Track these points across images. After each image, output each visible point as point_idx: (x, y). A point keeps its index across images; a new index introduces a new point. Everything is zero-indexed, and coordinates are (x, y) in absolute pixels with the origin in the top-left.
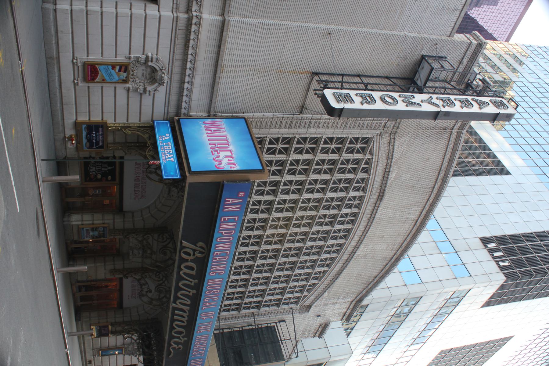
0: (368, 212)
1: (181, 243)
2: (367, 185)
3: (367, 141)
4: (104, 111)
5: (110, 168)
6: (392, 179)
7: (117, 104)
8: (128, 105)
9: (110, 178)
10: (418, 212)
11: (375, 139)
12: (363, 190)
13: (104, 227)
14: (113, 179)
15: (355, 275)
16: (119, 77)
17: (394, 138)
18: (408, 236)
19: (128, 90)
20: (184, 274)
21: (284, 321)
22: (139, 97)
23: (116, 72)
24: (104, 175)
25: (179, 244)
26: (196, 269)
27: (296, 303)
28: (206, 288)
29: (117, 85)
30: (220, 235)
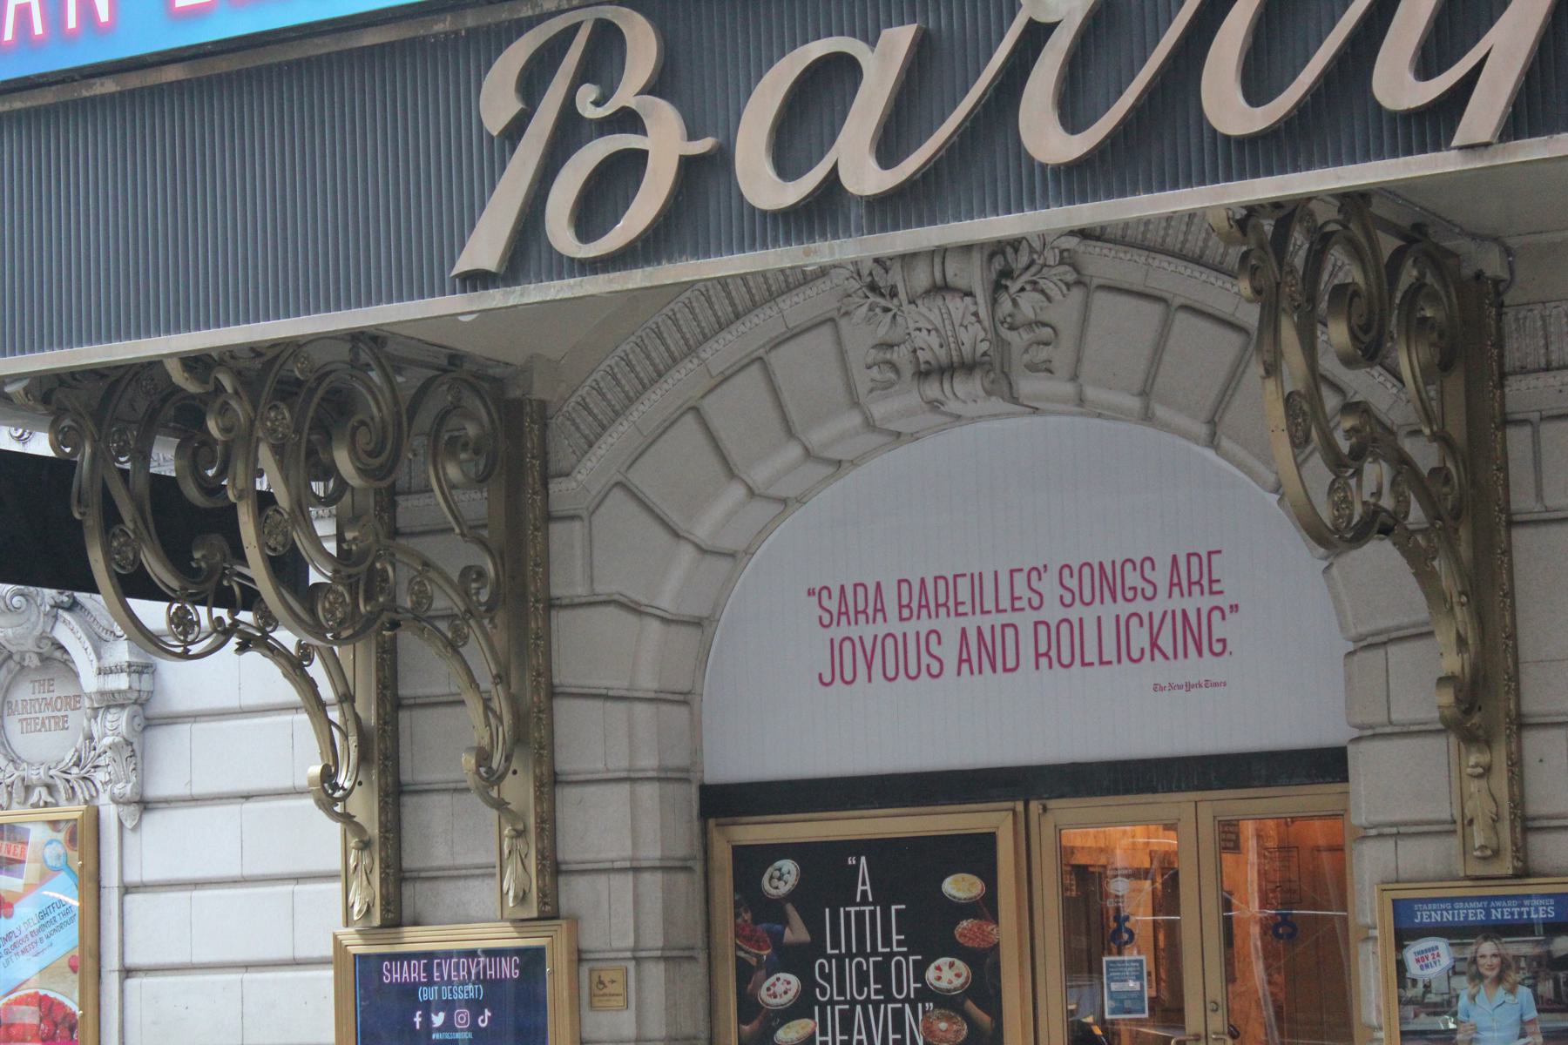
1: (477, 280)
4: (285, 953)
5: (864, 886)
7: (234, 871)
8: (247, 797)
9: (959, 887)
13: (1404, 934)
14: (976, 853)
16: (57, 870)
19: (144, 805)
20: (888, 148)
22: (183, 729)
23: (30, 888)
24: (932, 929)
25: (496, 298)
26: (817, 49)
29: (111, 878)
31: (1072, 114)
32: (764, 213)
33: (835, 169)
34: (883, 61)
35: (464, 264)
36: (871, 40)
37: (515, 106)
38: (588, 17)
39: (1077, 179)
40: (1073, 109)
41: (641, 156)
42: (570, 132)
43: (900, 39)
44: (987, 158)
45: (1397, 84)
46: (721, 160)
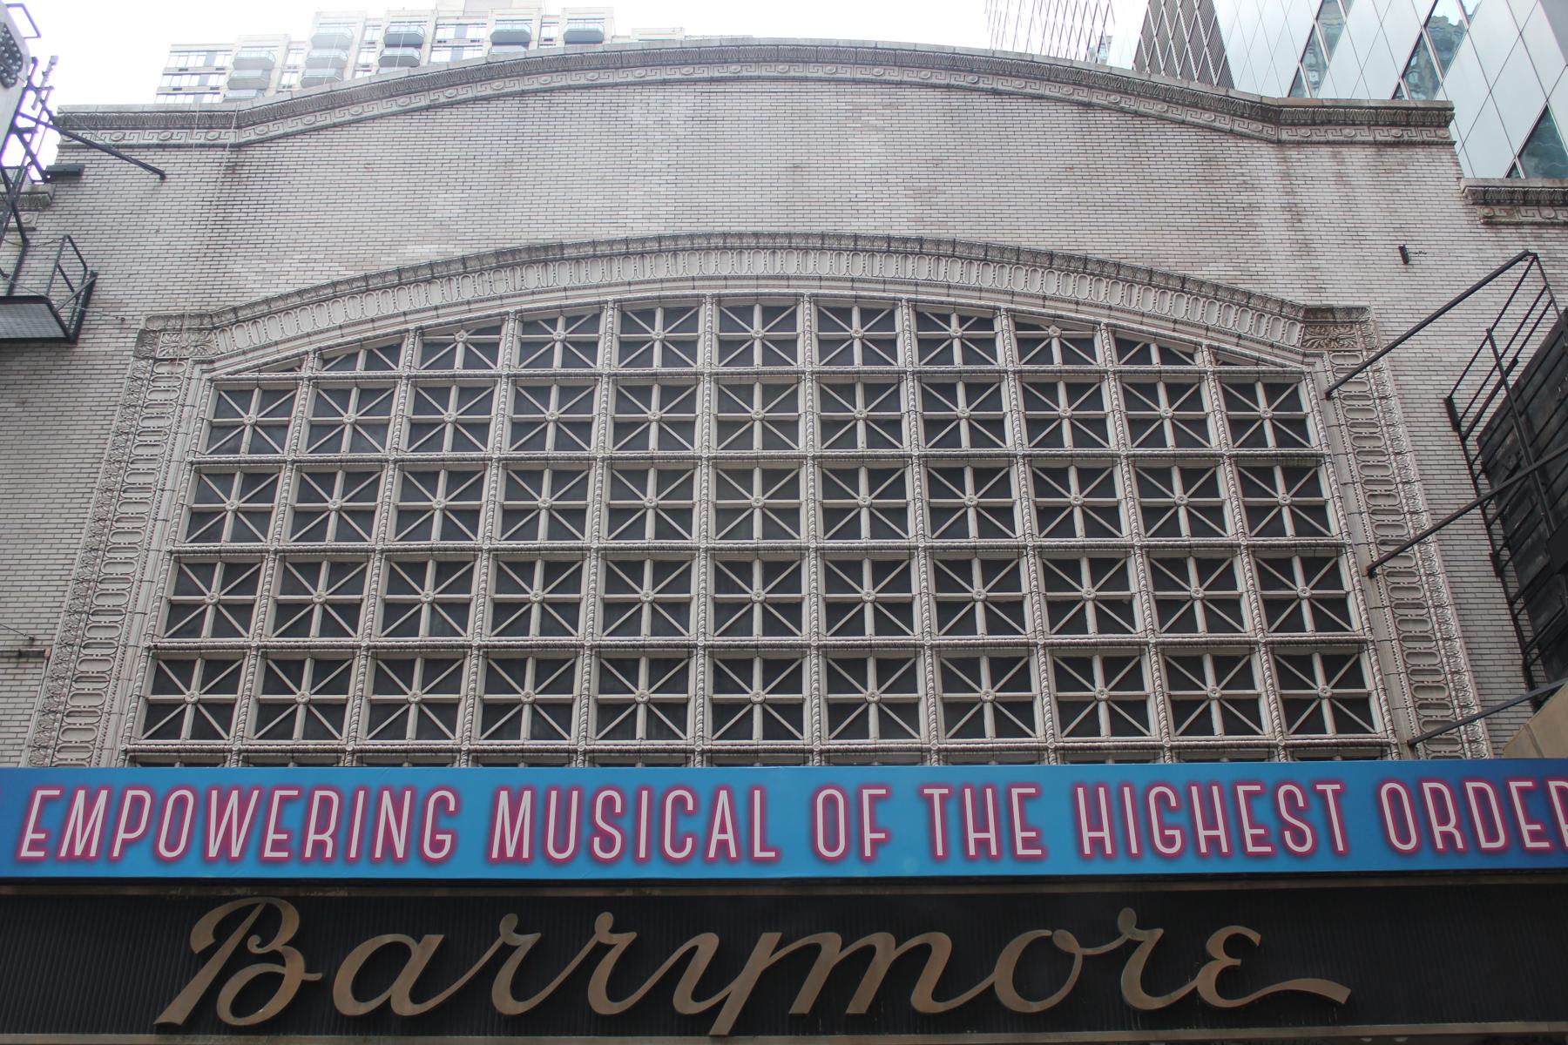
0: (596, 274)
2: (461, 325)
3: (232, 394)
6: (434, 247)
10: (655, 96)
11: (220, 374)
12: (497, 330)
15: (1066, 190)
17: (235, 310)
18: (806, 79)
20: (417, 995)
21: (1449, 402)
26: (388, 938)
27: (1282, 389)
28: (566, 861)
30: (143, 850)
31: (518, 992)
32: (344, 1017)
33: (388, 1001)
34: (423, 951)
35: (163, 1018)
36: (418, 941)
37: (211, 940)
38: (262, 903)
39: (517, 1025)
40: (519, 989)
41: (281, 977)
42: (241, 958)
43: (434, 941)
44: (470, 1009)
45: (684, 1002)
46: (325, 986)
